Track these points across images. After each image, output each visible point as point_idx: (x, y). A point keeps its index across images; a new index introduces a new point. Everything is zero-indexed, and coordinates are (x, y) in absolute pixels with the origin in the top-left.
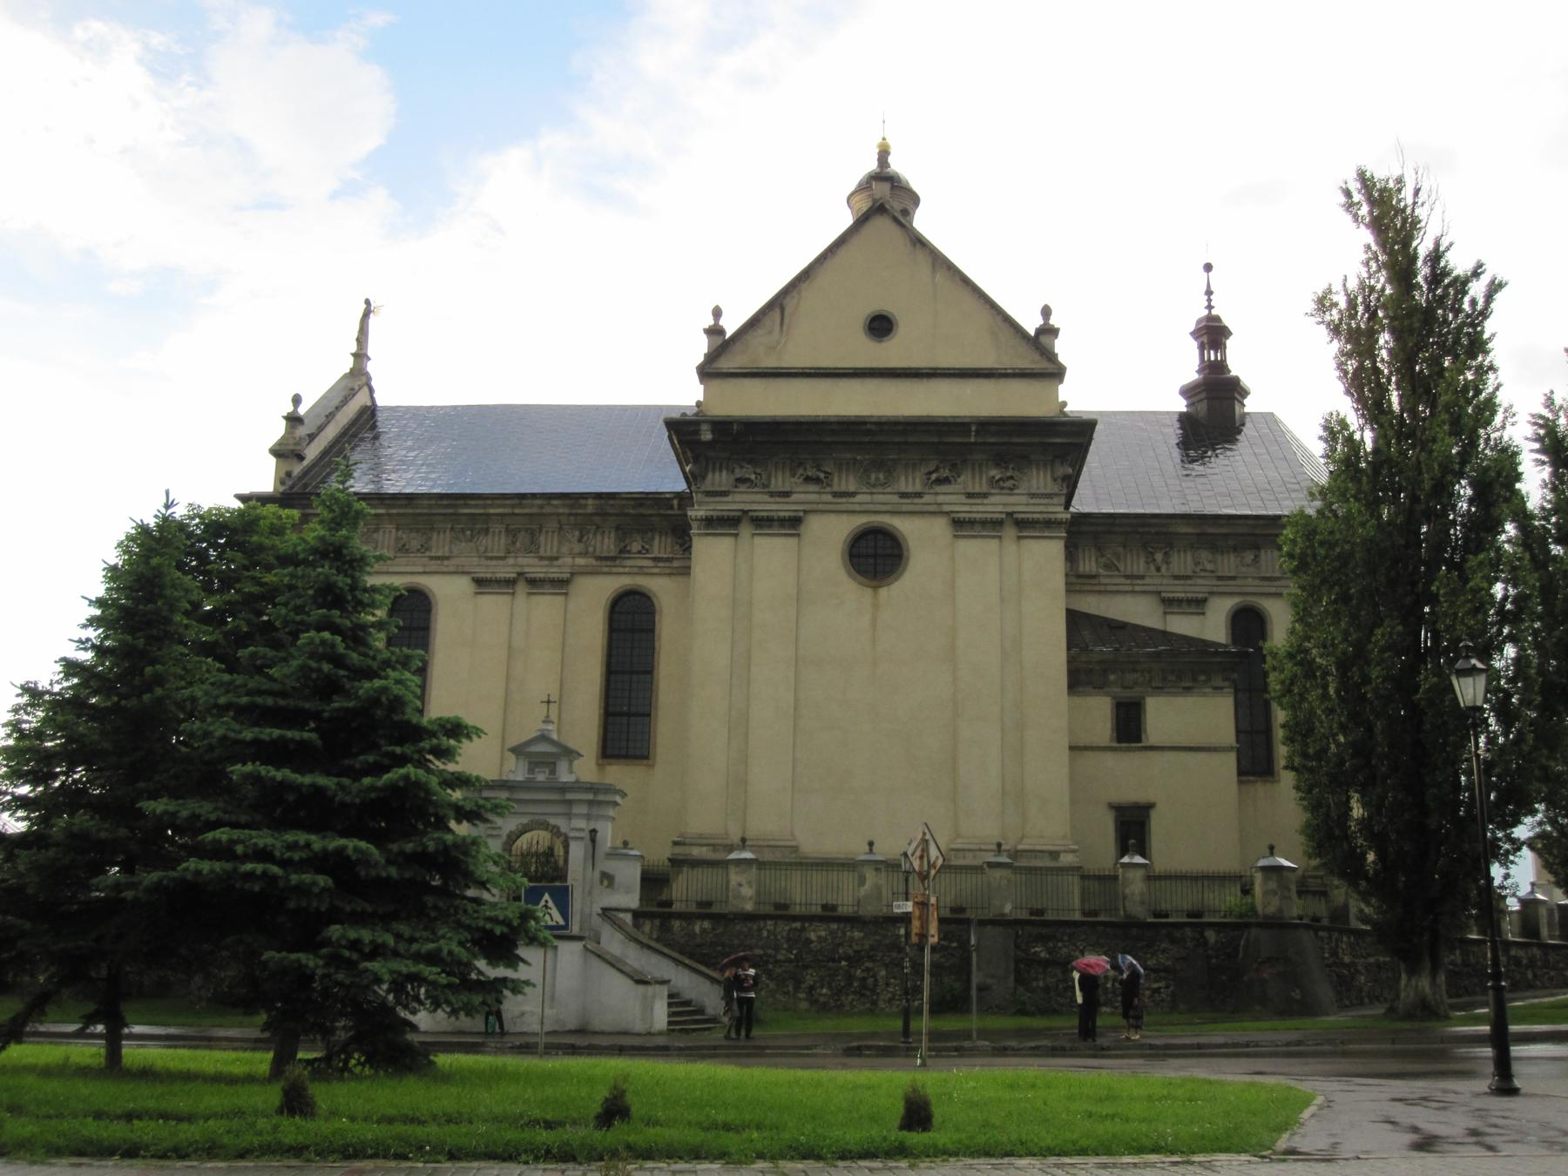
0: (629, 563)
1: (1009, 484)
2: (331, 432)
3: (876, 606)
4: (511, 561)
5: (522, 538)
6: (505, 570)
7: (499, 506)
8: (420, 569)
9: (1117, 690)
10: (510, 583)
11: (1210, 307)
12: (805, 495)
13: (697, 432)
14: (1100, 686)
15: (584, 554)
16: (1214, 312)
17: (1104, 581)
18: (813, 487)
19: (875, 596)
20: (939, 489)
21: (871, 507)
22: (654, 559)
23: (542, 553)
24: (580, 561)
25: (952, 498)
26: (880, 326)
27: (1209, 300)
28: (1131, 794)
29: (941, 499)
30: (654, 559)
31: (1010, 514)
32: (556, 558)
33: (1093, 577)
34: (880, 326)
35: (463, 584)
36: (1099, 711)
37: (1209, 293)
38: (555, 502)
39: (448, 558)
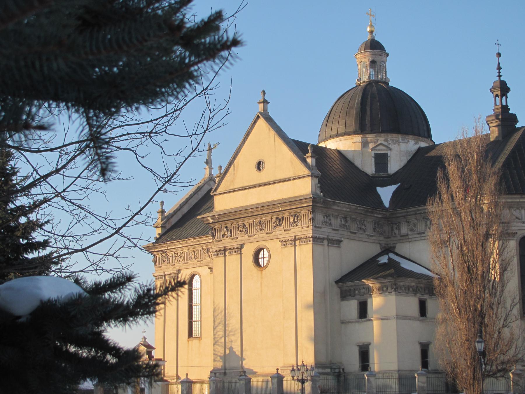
1: (295, 225)
2: (185, 209)
3: (262, 278)
9: (358, 297)
11: (500, 76)
12: (242, 238)
13: (208, 220)
14: (353, 296)
16: (502, 79)
17: (410, 237)
18: (243, 234)
19: (262, 273)
20: (277, 229)
21: (258, 239)
25: (279, 232)
26: (259, 166)
27: (499, 72)
28: (364, 340)
29: (277, 232)
31: (295, 237)
33: (407, 235)
34: (259, 166)
36: (352, 307)
37: (499, 68)
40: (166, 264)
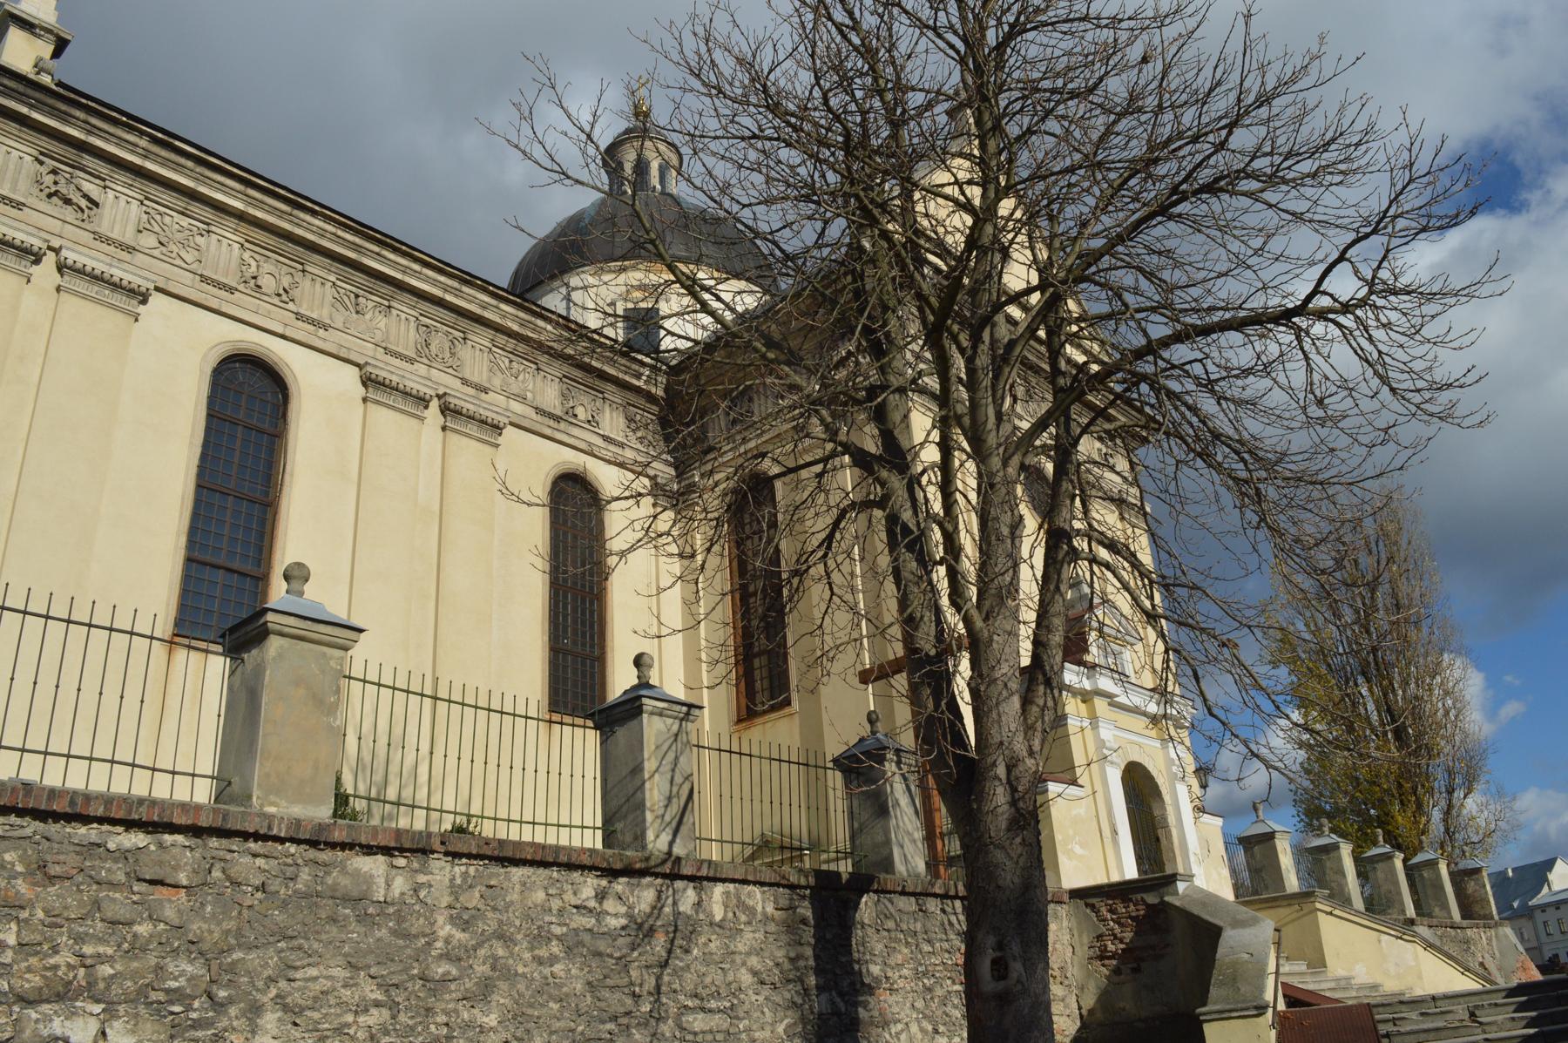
0: (575, 431)
4: (422, 369)
5: (438, 342)
6: (416, 377)
7: (427, 280)
8: (280, 330)
10: (423, 401)
15: (522, 399)
22: (606, 438)
23: (467, 376)
24: (517, 407)
30: (606, 438)
32: (486, 391)
35: (349, 377)
38: (503, 306)
39: (326, 327)
40: (69, 213)
